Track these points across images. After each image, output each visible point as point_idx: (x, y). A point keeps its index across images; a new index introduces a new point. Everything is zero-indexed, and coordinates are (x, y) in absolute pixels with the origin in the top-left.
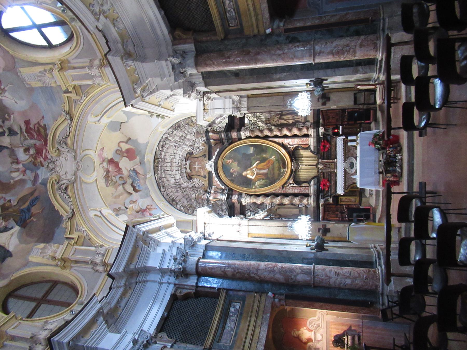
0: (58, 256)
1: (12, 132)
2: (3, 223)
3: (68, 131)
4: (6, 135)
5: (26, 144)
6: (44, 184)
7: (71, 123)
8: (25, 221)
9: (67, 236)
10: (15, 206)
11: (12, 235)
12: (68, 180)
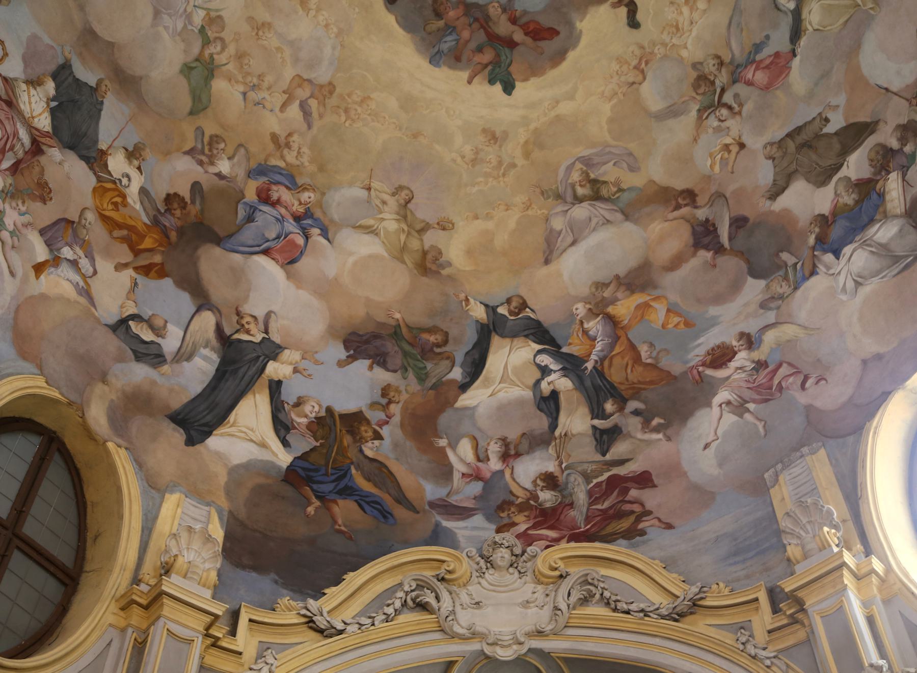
0: (173, 584)
1: (605, 438)
2: (304, 421)
3: (633, 607)
4: (596, 422)
5: (572, 479)
6: (436, 537)
7: (663, 617)
8: (309, 481)
9: (243, 610)
10: (361, 451)
11: (263, 445)
12: (453, 612)
